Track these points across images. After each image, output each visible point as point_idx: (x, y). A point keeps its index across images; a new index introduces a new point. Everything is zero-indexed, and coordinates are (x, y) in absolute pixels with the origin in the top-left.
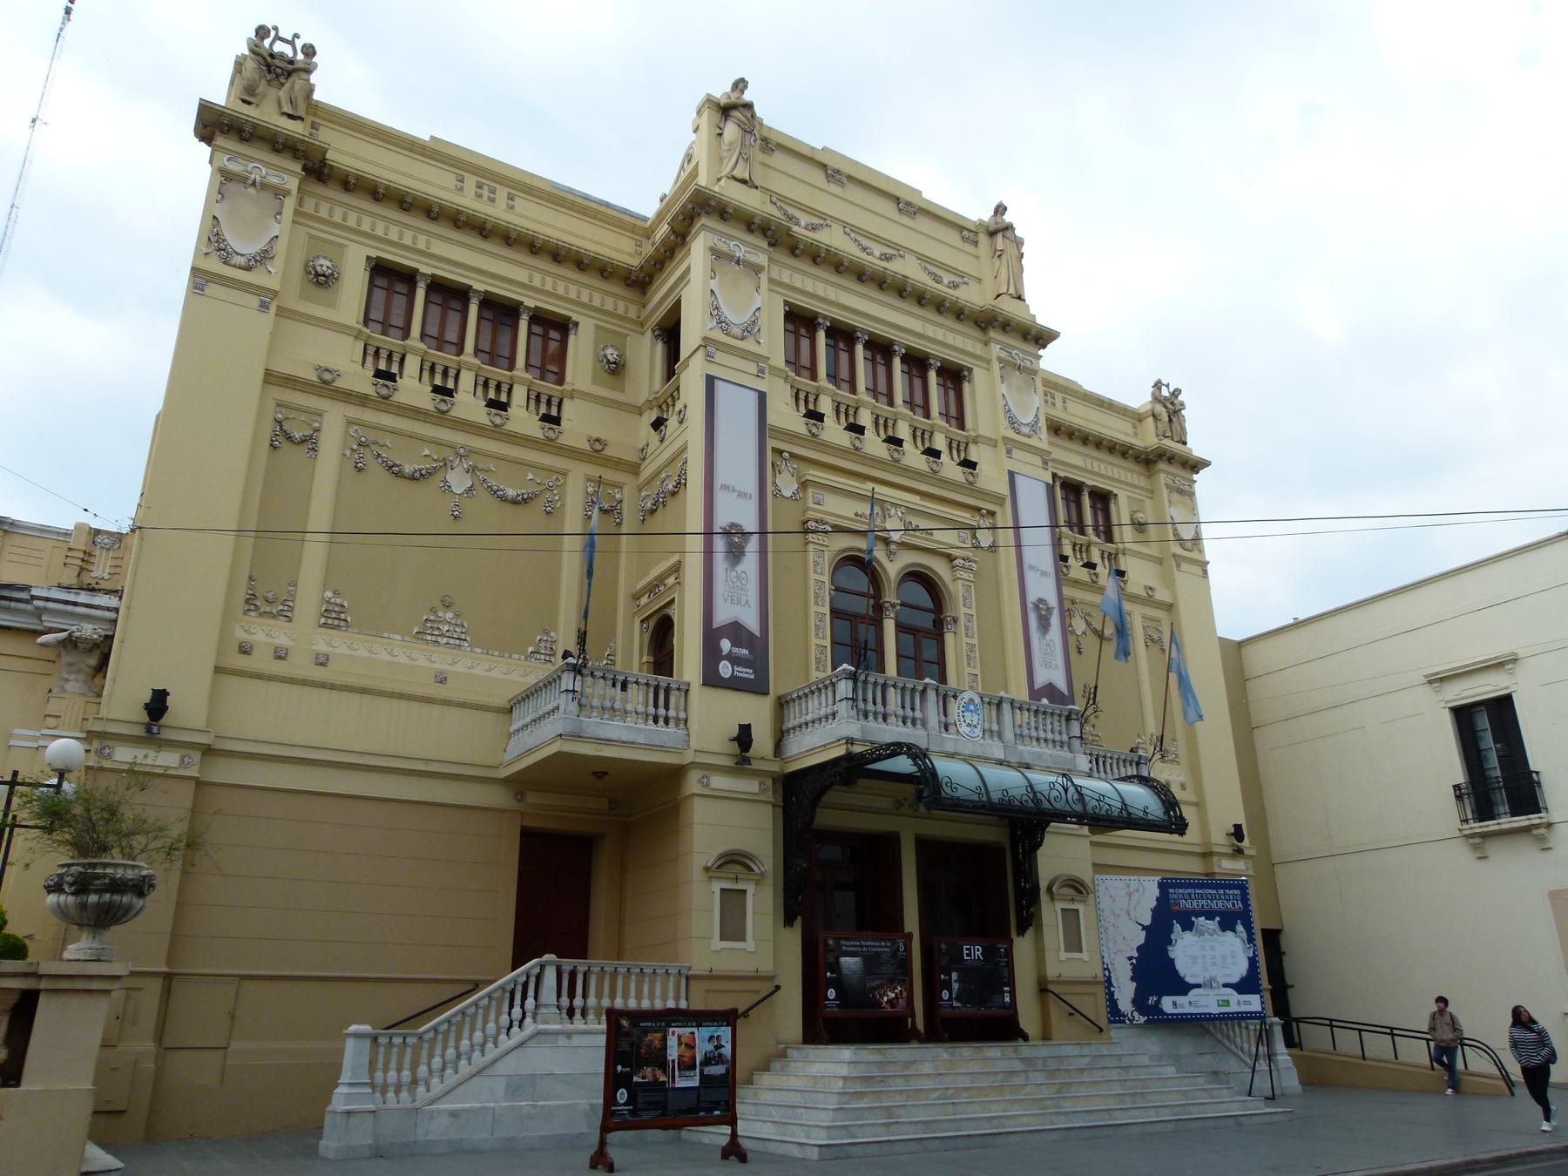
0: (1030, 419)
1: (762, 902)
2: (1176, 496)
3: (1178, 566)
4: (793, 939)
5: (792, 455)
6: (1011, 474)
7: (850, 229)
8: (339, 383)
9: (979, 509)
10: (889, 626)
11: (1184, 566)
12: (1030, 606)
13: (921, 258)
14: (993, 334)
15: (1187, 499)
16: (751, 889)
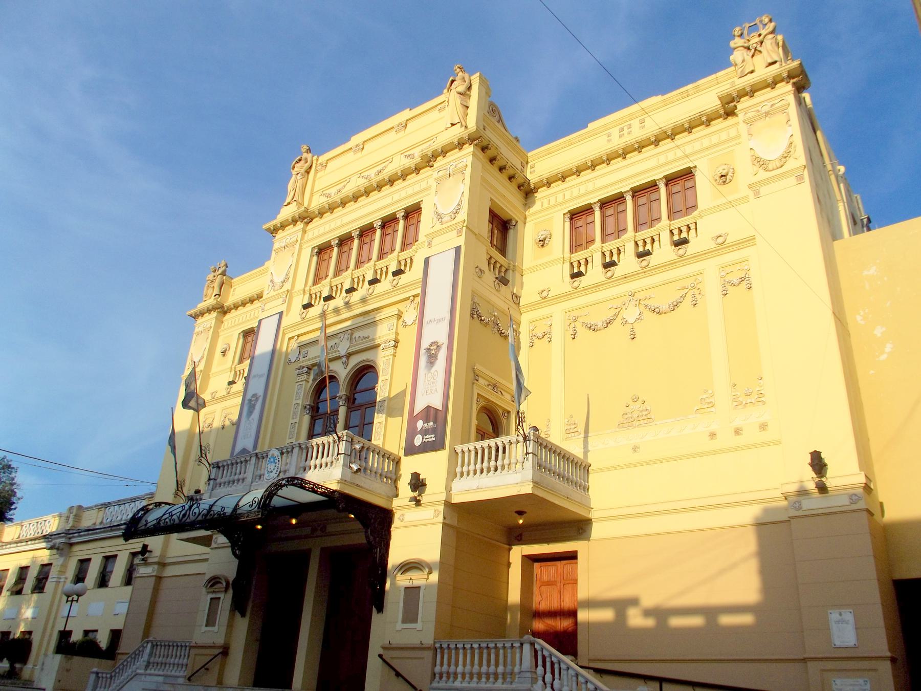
0: (453, 206)
1: (226, 600)
2: (759, 124)
3: (757, 195)
4: (242, 625)
5: (298, 336)
6: (427, 260)
7: (360, 174)
8: (217, 395)
9: (407, 299)
10: (342, 411)
11: (763, 190)
12: (423, 351)
13: (402, 153)
14: (436, 165)
15: (782, 118)
16: (221, 596)
